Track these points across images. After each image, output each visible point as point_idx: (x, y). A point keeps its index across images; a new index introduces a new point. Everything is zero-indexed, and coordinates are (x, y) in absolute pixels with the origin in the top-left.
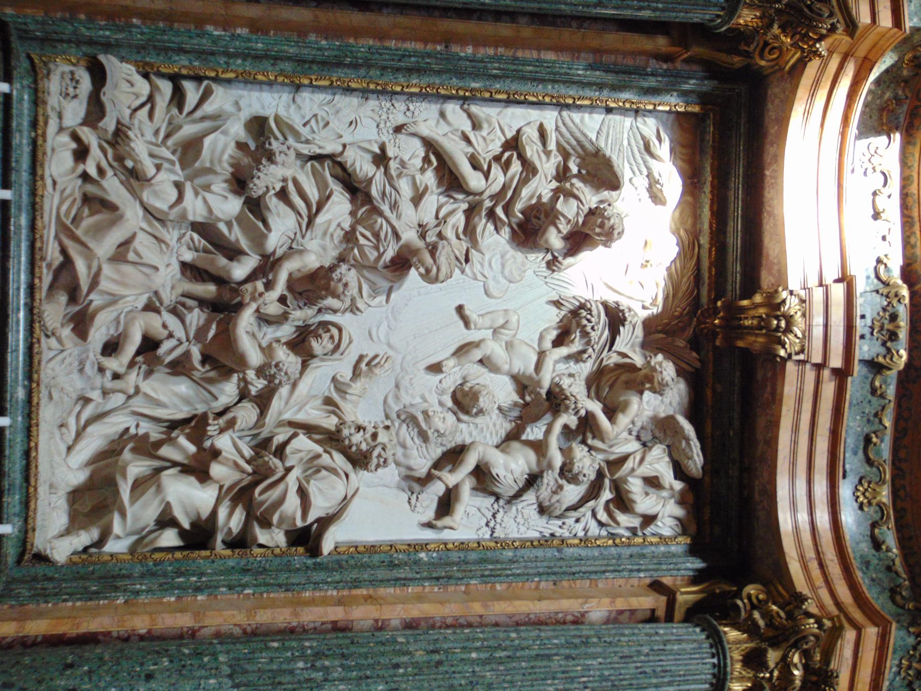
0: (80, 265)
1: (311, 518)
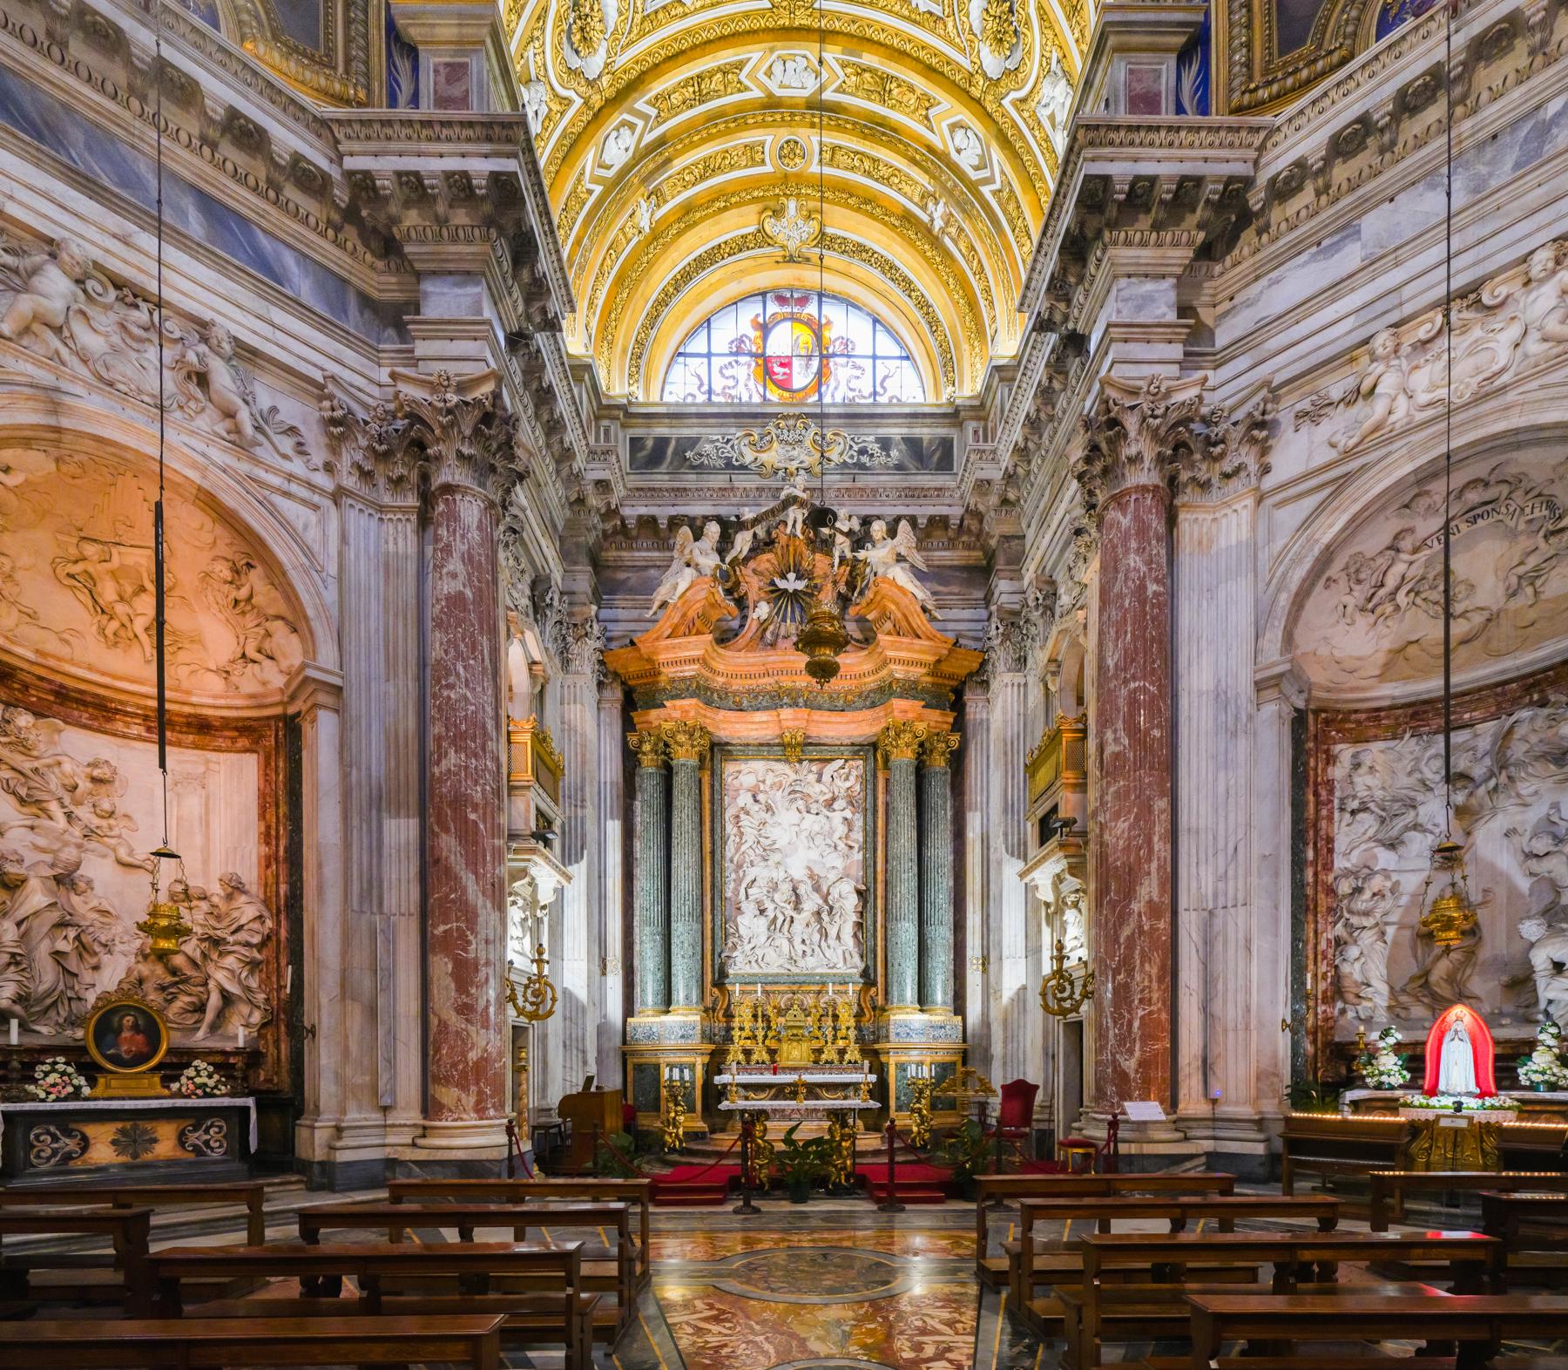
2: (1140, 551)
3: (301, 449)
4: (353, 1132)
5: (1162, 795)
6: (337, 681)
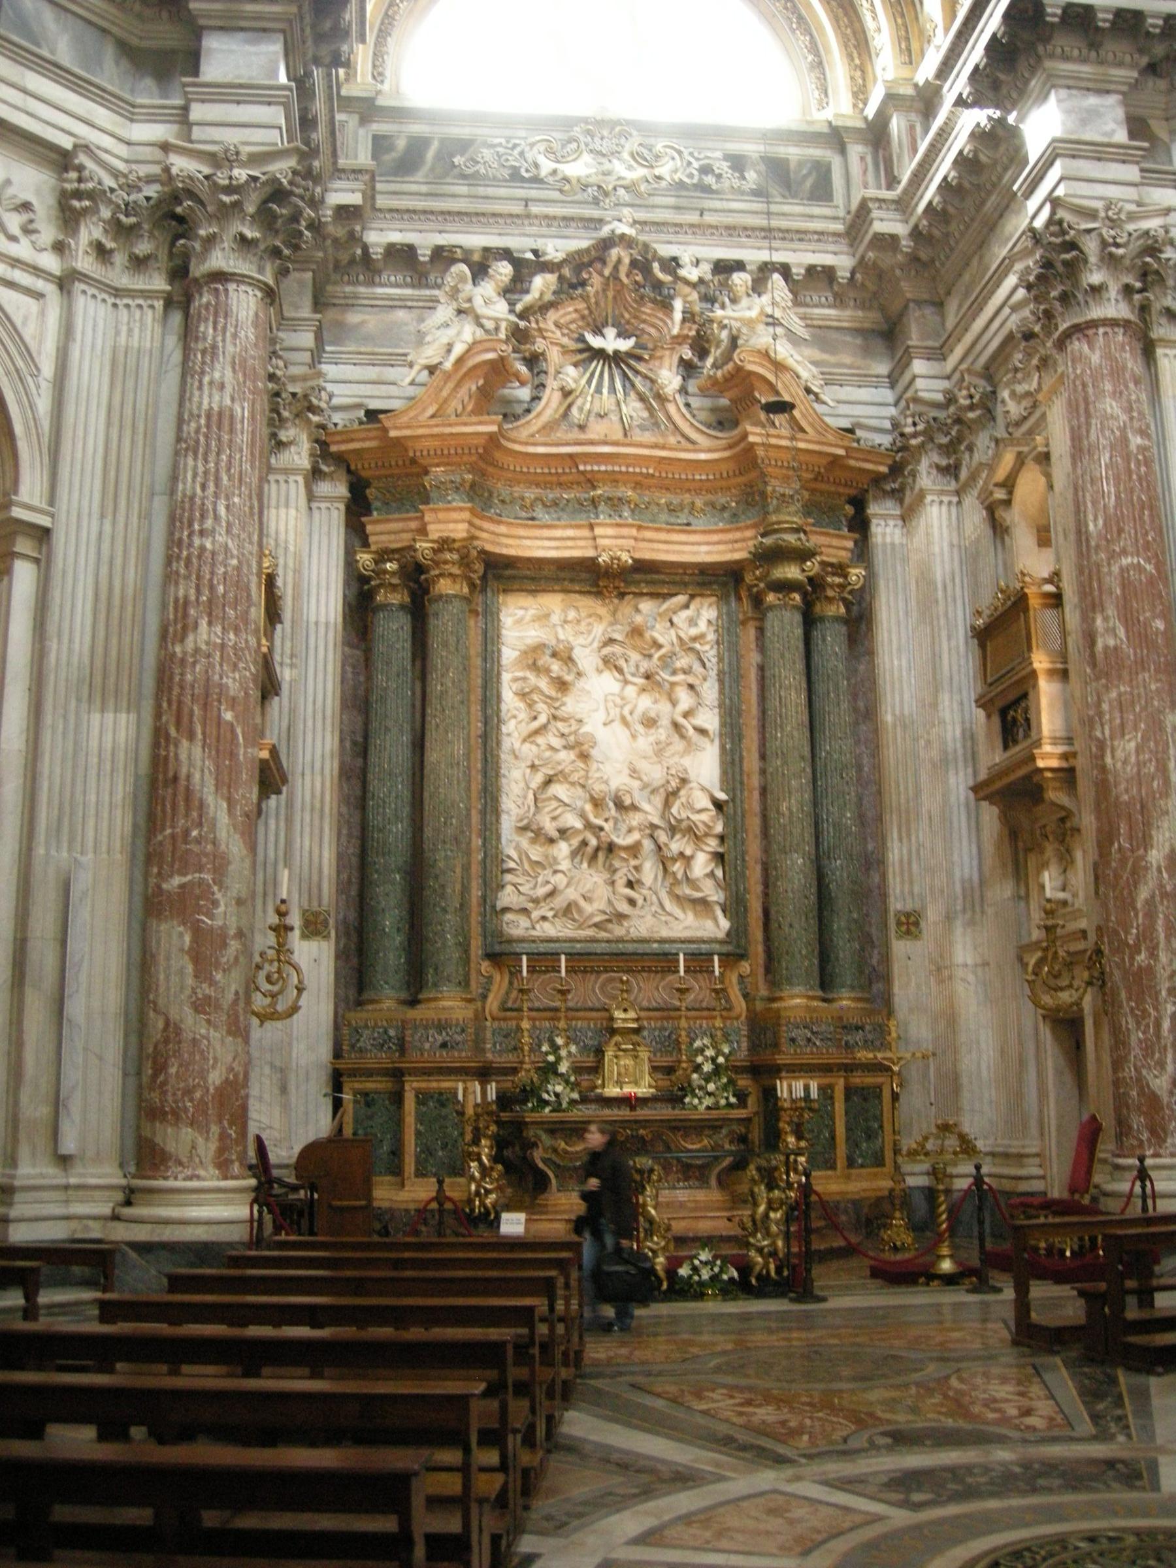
0: (597, 919)
1: (711, 807)
2: (1117, 394)
3: (27, 230)
4: (30, 1196)
6: (45, 521)
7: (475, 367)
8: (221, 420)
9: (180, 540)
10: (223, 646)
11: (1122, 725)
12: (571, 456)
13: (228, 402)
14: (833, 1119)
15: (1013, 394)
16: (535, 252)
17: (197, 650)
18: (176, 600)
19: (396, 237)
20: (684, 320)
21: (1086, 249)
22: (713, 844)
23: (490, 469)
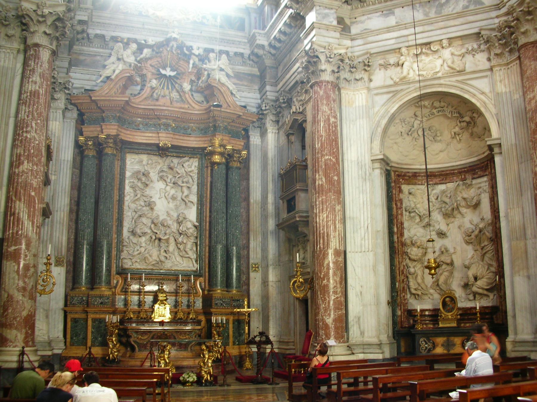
0: (154, 263)
1: (193, 227)
5: (339, 203)
7: (122, 78)
8: (35, 94)
9: (19, 134)
10: (32, 170)
11: (323, 209)
12: (152, 109)
13: (37, 88)
14: (229, 330)
15: (297, 100)
16: (145, 41)
17: (23, 171)
18: (17, 154)
19: (98, 32)
20: (193, 67)
21: (321, 58)
22: (192, 240)
23: (125, 112)
